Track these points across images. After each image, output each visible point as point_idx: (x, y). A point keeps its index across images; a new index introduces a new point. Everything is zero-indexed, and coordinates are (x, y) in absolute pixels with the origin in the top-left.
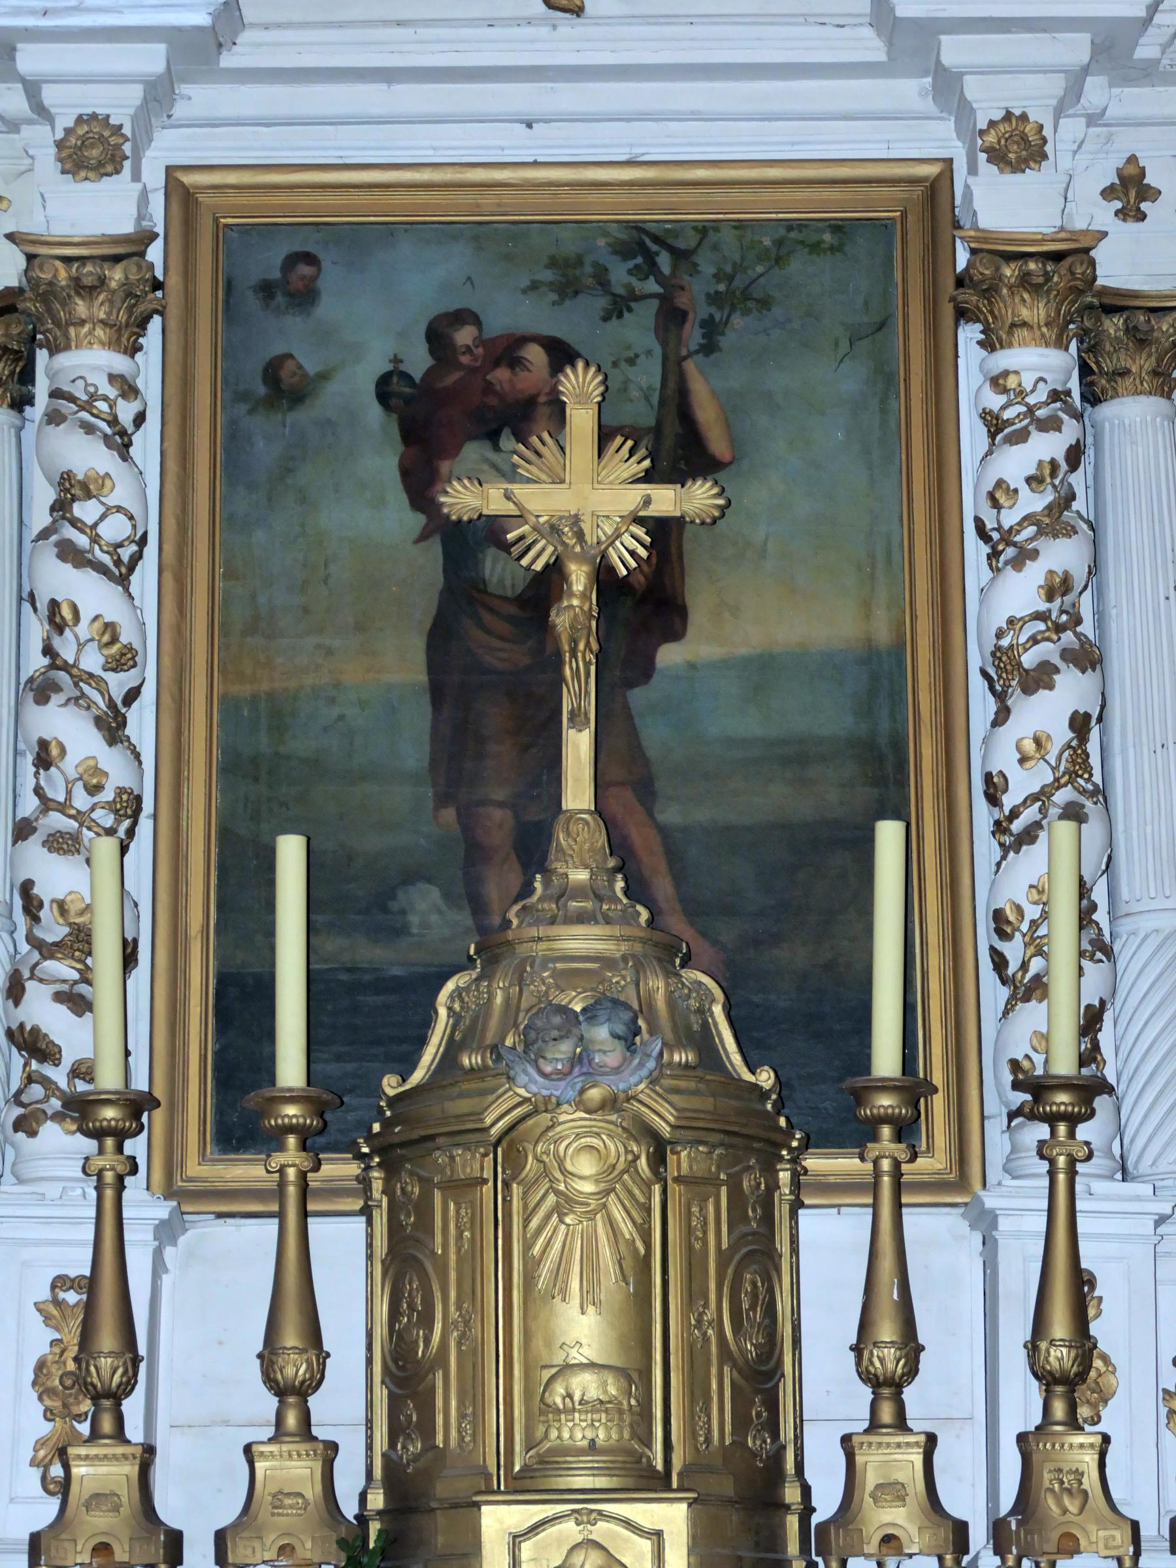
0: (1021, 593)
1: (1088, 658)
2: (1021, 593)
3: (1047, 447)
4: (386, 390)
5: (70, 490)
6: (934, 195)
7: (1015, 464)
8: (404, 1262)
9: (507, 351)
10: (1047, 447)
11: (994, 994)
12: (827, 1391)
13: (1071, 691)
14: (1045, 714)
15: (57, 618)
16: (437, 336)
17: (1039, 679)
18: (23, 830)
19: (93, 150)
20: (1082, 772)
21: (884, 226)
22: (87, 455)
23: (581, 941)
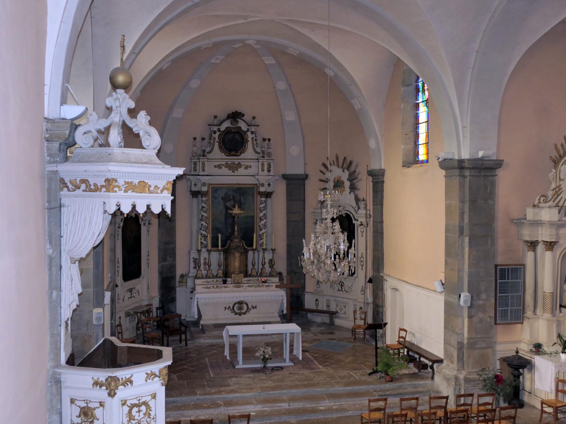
0: (262, 214)
1: (265, 218)
2: (262, 214)
3: (264, 205)
4: (222, 198)
5: (203, 207)
6: (256, 185)
7: (262, 206)
8: (226, 259)
9: (230, 196)
10: (264, 205)
11: (259, 239)
12: (250, 267)
13: (265, 221)
14: (263, 222)
15: (203, 216)
16: (225, 194)
17: (263, 220)
18: (201, 229)
19: (204, 184)
20: (265, 225)
21: (253, 188)
22: (204, 205)
23: (236, 240)
